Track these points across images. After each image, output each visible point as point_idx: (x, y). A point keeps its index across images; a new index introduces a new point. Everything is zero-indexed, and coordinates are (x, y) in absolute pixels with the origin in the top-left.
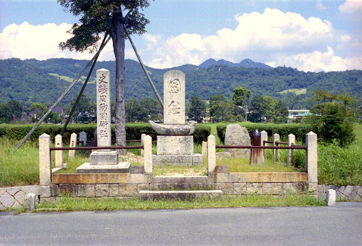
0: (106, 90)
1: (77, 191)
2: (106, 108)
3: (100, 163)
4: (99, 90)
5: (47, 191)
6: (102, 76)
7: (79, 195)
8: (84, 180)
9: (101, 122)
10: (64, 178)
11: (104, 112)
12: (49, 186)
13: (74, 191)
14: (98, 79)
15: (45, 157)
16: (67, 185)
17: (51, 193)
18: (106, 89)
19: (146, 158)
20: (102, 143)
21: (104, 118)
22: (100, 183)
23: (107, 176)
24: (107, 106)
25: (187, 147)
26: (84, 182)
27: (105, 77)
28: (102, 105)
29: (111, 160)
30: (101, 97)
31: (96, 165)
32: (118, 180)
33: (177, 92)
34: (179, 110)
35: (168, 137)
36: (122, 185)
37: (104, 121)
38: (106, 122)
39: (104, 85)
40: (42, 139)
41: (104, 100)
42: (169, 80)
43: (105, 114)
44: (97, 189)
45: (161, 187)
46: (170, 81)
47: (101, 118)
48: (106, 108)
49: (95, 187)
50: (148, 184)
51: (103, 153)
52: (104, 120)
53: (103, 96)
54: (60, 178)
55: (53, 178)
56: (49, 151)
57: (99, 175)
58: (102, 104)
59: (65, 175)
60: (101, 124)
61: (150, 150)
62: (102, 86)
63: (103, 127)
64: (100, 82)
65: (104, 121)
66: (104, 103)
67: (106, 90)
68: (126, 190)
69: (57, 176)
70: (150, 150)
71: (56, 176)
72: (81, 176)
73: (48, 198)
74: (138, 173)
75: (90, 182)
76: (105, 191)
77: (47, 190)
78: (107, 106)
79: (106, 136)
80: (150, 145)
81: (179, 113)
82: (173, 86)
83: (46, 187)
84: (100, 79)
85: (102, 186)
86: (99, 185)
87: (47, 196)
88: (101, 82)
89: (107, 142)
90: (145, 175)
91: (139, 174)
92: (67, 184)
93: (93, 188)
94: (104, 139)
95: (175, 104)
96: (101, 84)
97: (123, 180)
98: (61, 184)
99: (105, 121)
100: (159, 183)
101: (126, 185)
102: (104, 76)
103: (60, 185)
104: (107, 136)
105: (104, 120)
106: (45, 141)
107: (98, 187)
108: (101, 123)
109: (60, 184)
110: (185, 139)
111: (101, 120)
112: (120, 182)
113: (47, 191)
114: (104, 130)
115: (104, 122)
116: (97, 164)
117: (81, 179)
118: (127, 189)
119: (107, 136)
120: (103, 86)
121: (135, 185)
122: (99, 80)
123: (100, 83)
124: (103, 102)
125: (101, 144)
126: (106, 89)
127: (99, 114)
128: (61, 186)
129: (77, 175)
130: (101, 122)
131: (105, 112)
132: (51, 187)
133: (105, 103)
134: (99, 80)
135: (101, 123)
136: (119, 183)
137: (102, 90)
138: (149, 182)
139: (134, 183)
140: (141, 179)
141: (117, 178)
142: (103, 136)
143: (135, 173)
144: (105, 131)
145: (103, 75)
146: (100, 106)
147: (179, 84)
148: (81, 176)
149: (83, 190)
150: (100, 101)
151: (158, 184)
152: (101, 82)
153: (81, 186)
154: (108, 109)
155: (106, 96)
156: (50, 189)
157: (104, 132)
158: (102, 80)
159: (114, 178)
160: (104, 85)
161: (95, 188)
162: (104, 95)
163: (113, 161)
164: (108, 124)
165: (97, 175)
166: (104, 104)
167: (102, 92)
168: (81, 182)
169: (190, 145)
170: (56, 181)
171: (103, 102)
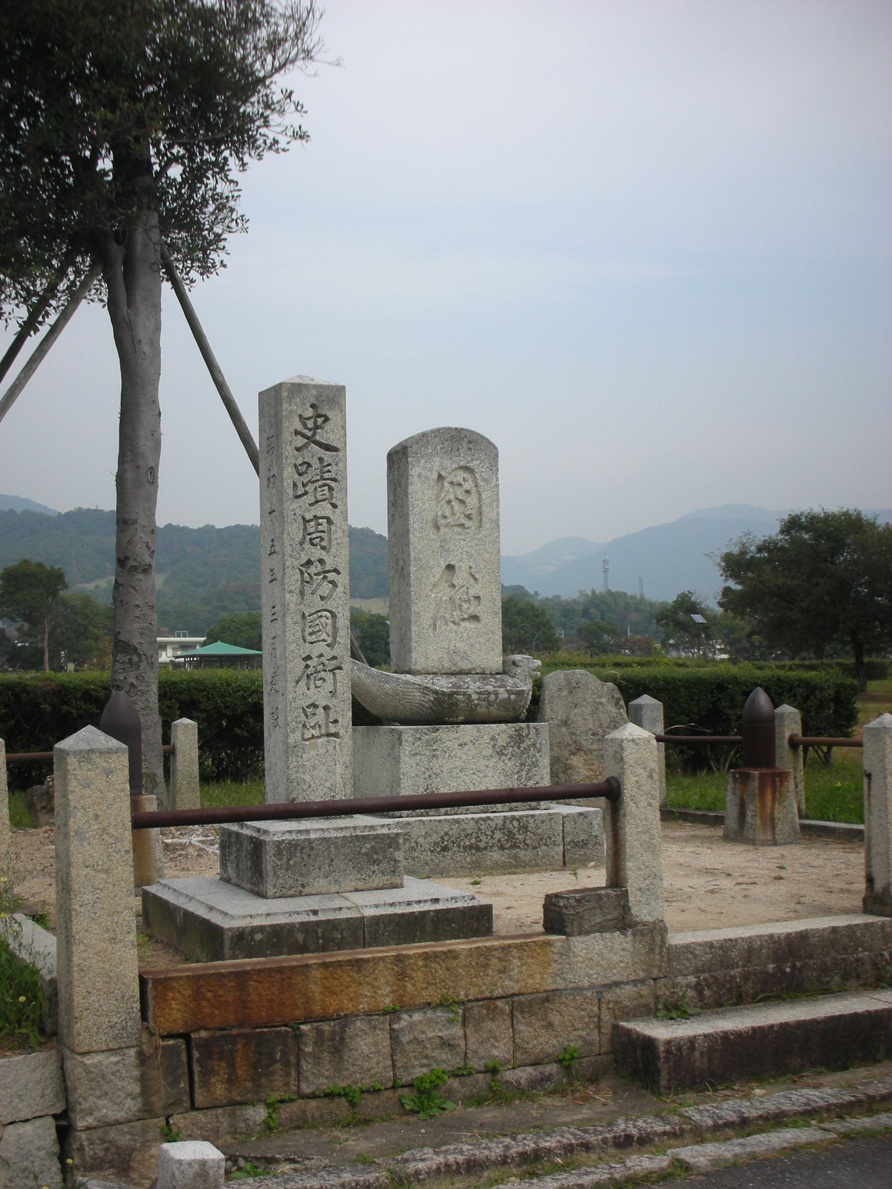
0: (331, 489)
1: (298, 1064)
2: (331, 582)
3: (321, 883)
4: (295, 485)
5: (120, 1084)
6: (310, 412)
7: (306, 1089)
8: (333, 993)
9: (308, 658)
10: (221, 992)
11: (321, 605)
12: (132, 1052)
13: (278, 1066)
14: (292, 430)
15: (107, 872)
16: (238, 1035)
17: (146, 1092)
18: (333, 484)
19: (636, 843)
20: (315, 773)
21: (324, 636)
22: (418, 1000)
23: (456, 958)
24: (336, 571)
25: (524, 773)
26: (333, 1004)
27: (327, 419)
28: (313, 570)
29: (377, 862)
30: (306, 521)
31: (301, 894)
32: (510, 978)
33: (468, 523)
34: (473, 609)
35: (445, 733)
36: (531, 1004)
37: (321, 655)
38: (334, 658)
39: (321, 460)
40: (88, 760)
41: (322, 539)
42: (431, 470)
43: (328, 614)
44: (405, 1039)
45: (707, 993)
46: (435, 476)
47: (309, 639)
48: (331, 582)
49: (395, 1026)
50: (652, 982)
51: (336, 829)
52: (321, 648)
53: (316, 517)
54: (197, 996)
55: (155, 998)
56: (128, 834)
57: (409, 956)
58: (309, 563)
59: (222, 976)
60: (311, 670)
61: (650, 805)
62: (309, 465)
63: (319, 683)
64: (300, 441)
65: (321, 655)
66: (323, 554)
67: (331, 489)
68: (550, 1025)
69: (175, 985)
70: (650, 805)
71: (173, 989)
72: (317, 974)
73: (125, 1128)
74: (601, 928)
75: (363, 1006)
76: (447, 1044)
77: (122, 1079)
78: (336, 571)
79: (329, 735)
80: (651, 777)
81: (475, 618)
82: (452, 497)
83: (114, 1059)
84: (298, 426)
85: (430, 1020)
86: (417, 1016)
87: (121, 1115)
88: (305, 446)
89: (339, 769)
90: (634, 935)
91: (607, 935)
92: (235, 1032)
93: (383, 1037)
94: (322, 751)
95: (461, 577)
96: (307, 456)
97: (531, 976)
98: (203, 1034)
99: (329, 653)
100: (697, 971)
101: (549, 997)
102: (320, 412)
103: (194, 1036)
104: (336, 735)
105: (321, 648)
106: (108, 773)
107: (411, 1026)
108: (307, 666)
109: (197, 1030)
110: (519, 738)
111: (307, 649)
112: (516, 990)
113: (120, 1084)
114: (322, 703)
115: (323, 659)
116: (307, 890)
117: (315, 990)
118: (555, 1019)
119: (336, 735)
120: (316, 464)
121: (589, 994)
122: (297, 433)
123: (298, 449)
124: (317, 553)
125: (307, 777)
126: (333, 484)
127: (298, 618)
128: (206, 1045)
129: (292, 968)
130: (308, 658)
131: (330, 605)
132: (143, 1059)
133: (325, 558)
134: (297, 433)
135: (307, 666)
136: (513, 995)
137: (310, 488)
138: (655, 973)
139: (587, 984)
140: (616, 958)
141: (499, 966)
142: (316, 732)
143: (588, 933)
144: (326, 708)
145: (313, 406)
146: (302, 573)
147: (474, 491)
148: (317, 974)
149: (326, 1056)
150: (301, 543)
151: (692, 979)
152: (305, 446)
153: (320, 1033)
154: (340, 589)
155: (329, 521)
156: (136, 1073)
157: (320, 711)
158: (309, 434)
159: (486, 966)
160: (321, 460)
161: (394, 1036)
162: (322, 514)
163: (384, 865)
164: (340, 668)
165: (399, 959)
166: (321, 561)
167: (310, 499)
168: (317, 1009)
169: (535, 765)
170: (175, 1014)
171: (317, 553)
